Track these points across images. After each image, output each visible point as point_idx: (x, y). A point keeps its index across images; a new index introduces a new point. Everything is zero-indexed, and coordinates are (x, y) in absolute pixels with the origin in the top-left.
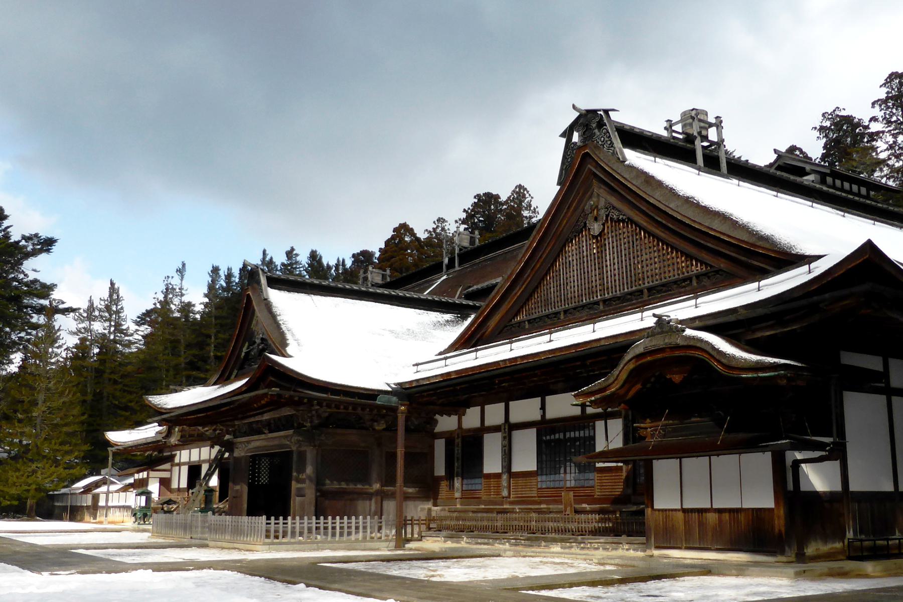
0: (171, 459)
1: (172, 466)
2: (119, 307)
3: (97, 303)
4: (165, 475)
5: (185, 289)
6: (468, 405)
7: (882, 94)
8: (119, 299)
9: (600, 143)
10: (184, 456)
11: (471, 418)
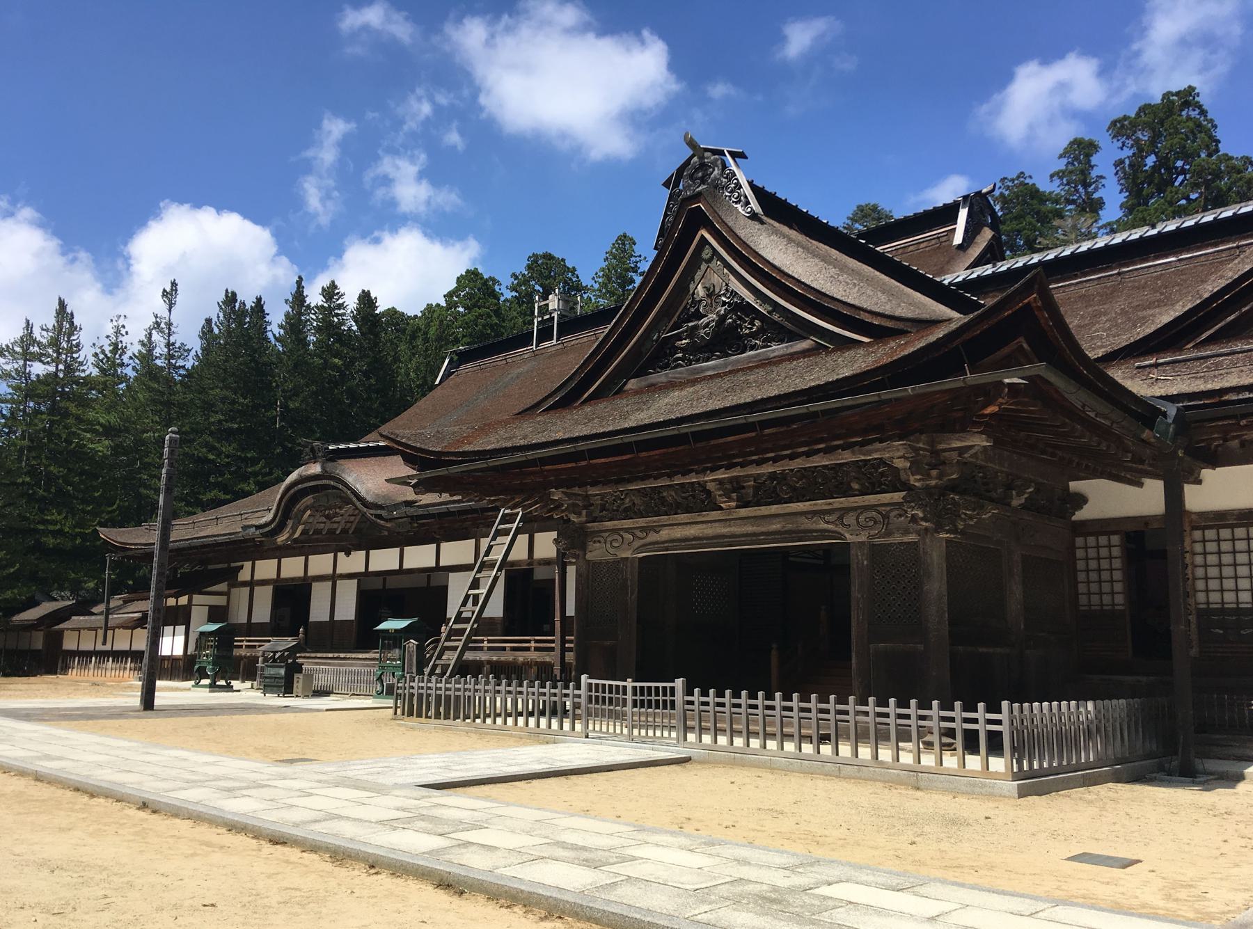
0: (230, 575)
3: (37, 334)
7: (1061, 165)
8: (73, 328)
10: (266, 569)
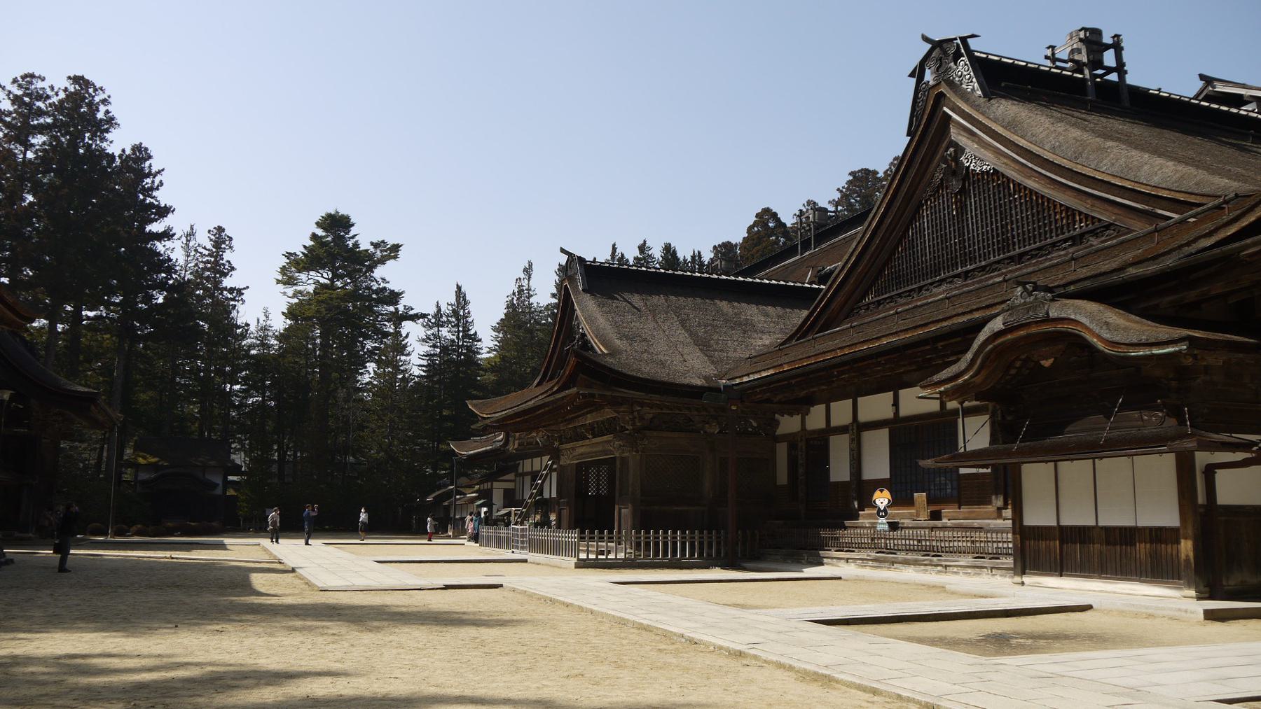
0: (514, 469)
1: (516, 476)
2: (466, 311)
3: (444, 308)
4: (510, 485)
5: (533, 289)
6: (810, 401)
8: (466, 303)
9: (957, 79)
11: (816, 418)
